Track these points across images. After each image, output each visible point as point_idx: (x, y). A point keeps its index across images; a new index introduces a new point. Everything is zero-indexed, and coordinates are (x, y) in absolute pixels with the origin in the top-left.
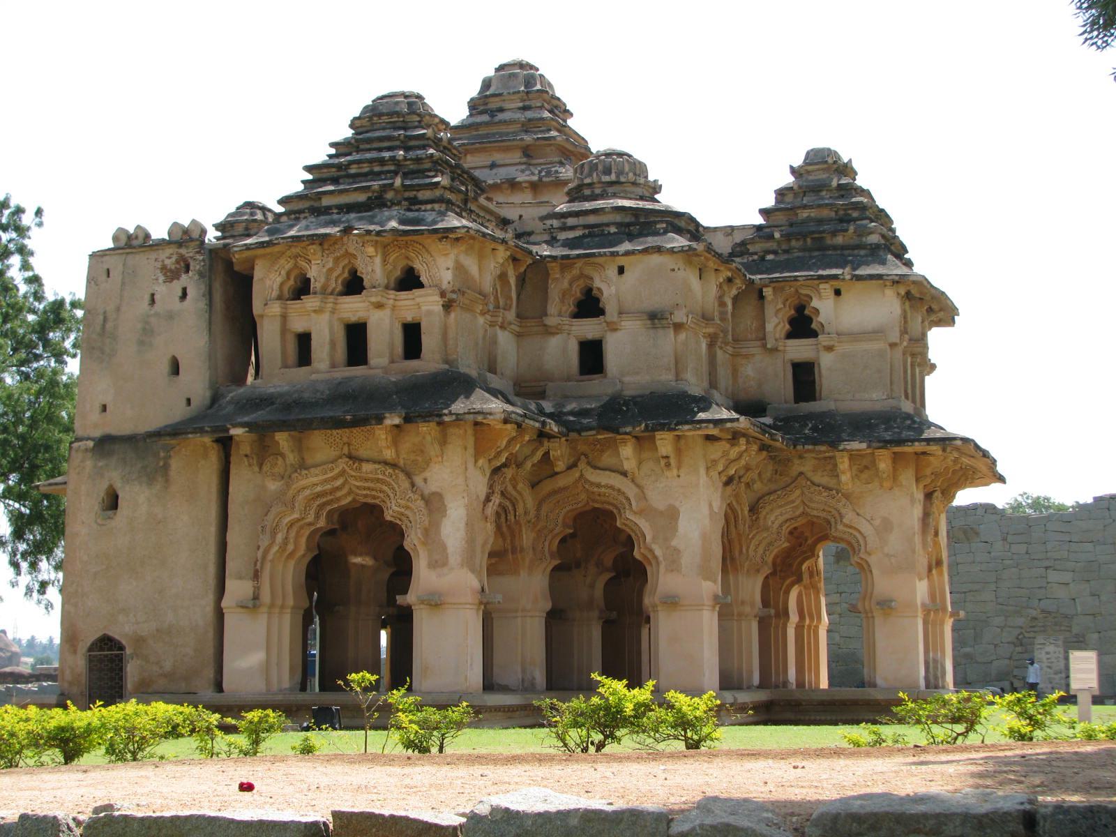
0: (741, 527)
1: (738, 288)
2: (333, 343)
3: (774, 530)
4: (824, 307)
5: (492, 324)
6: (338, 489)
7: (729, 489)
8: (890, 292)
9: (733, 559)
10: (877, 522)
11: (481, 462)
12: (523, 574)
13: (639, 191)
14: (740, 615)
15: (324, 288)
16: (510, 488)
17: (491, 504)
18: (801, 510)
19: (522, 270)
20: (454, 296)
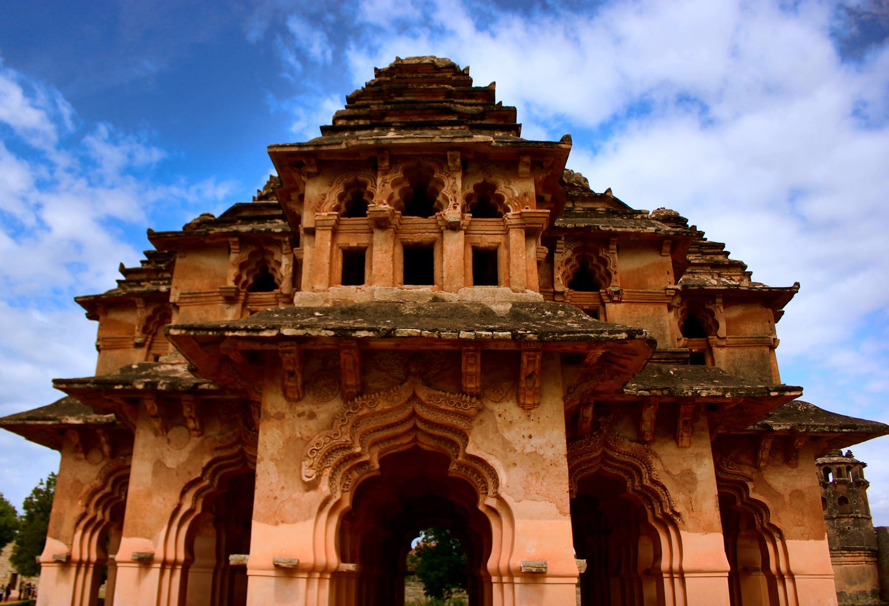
1: (285, 242)
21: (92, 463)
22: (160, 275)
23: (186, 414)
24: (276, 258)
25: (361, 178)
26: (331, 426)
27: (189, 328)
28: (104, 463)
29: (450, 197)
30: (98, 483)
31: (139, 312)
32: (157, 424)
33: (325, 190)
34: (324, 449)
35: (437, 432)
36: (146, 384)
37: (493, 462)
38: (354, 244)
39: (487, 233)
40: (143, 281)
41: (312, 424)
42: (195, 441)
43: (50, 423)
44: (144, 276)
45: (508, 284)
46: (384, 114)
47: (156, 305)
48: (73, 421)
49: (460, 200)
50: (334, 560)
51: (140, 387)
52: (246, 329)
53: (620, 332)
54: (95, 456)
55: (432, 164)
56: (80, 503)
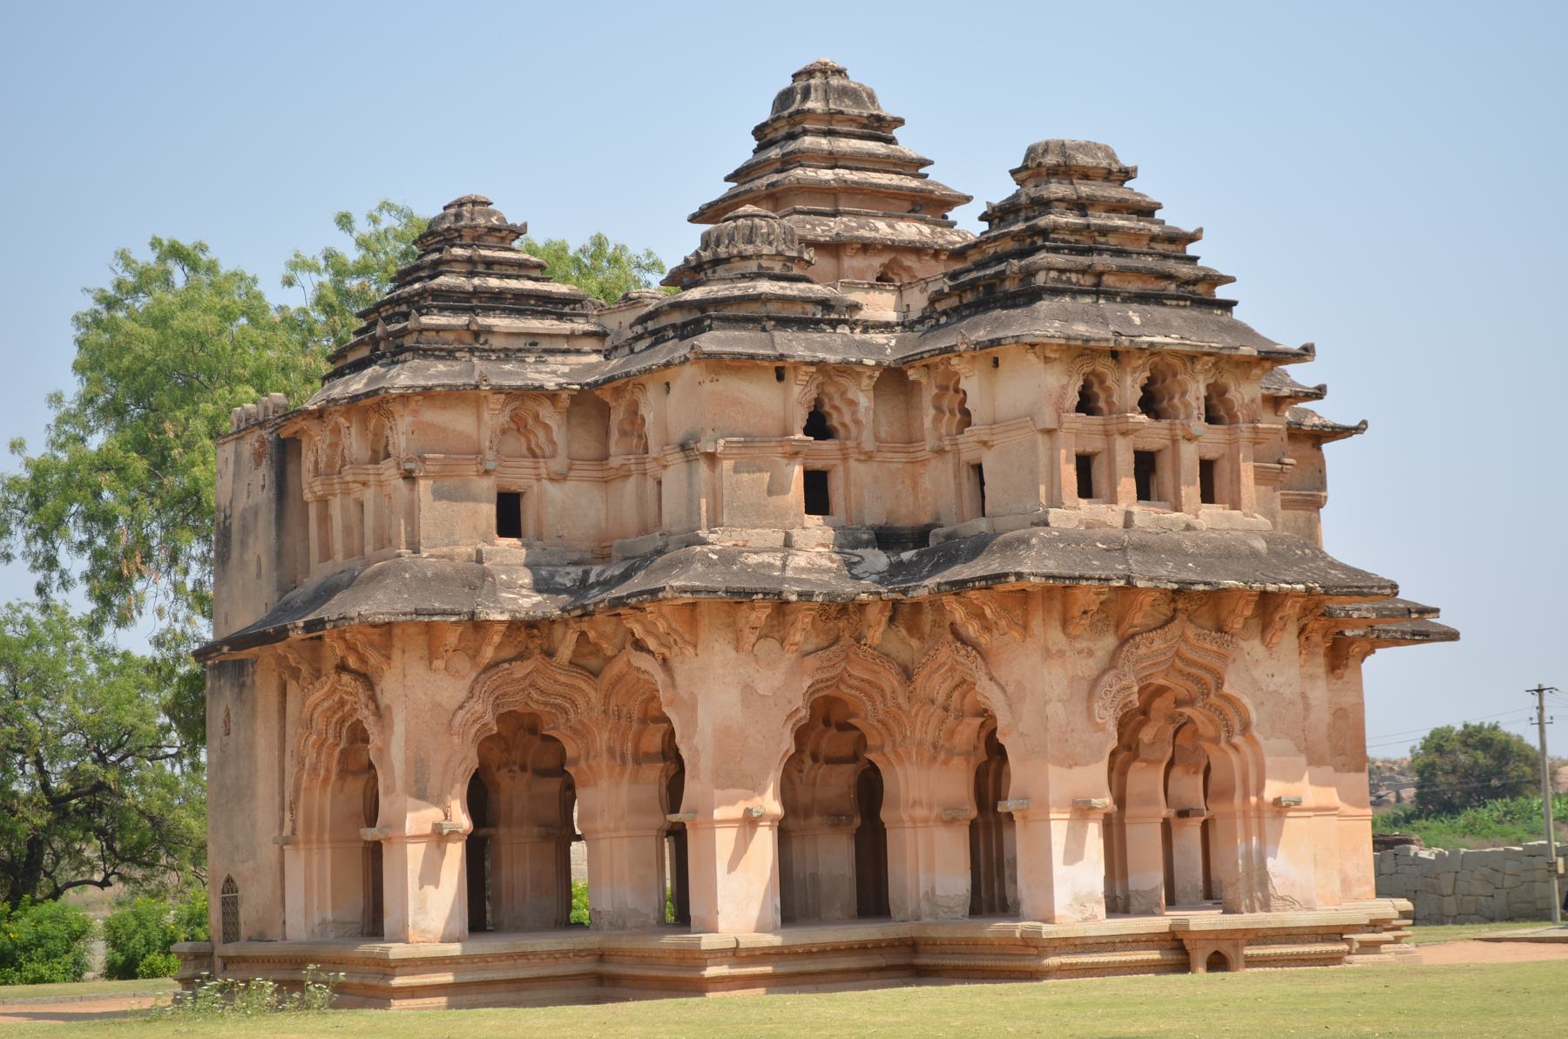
0: (890, 704)
1: (871, 377)
2: (347, 530)
3: (940, 699)
4: (972, 384)
5: (539, 480)
6: (342, 703)
7: (811, 662)
8: (1031, 357)
9: (894, 742)
10: (1011, 689)
11: (439, 664)
12: (604, 784)
13: (752, 266)
14: (914, 820)
15: (330, 464)
16: (540, 682)
17: (462, 712)
18: (957, 679)
19: (567, 403)
20: (409, 466)
21: (457, 674)
22: (482, 340)
23: (799, 625)
24: (850, 395)
25: (1100, 369)
26: (1112, 662)
27: (1048, 577)
28: (474, 675)
29: (1194, 404)
30: (479, 707)
31: (486, 416)
32: (753, 639)
33: (1064, 380)
34: (1115, 688)
35: (1193, 670)
36: (800, 595)
37: (1247, 701)
38: (1089, 449)
39: (1211, 440)
40: (460, 350)
41: (1091, 662)
42: (790, 656)
43: (454, 619)
44: (451, 337)
45: (1236, 505)
46: (1100, 275)
47: (517, 404)
48: (496, 616)
49: (1203, 410)
50: (1105, 801)
51: (794, 598)
52: (1100, 579)
53: (1384, 587)
54: (462, 663)
55: (1176, 362)
56: (456, 740)
